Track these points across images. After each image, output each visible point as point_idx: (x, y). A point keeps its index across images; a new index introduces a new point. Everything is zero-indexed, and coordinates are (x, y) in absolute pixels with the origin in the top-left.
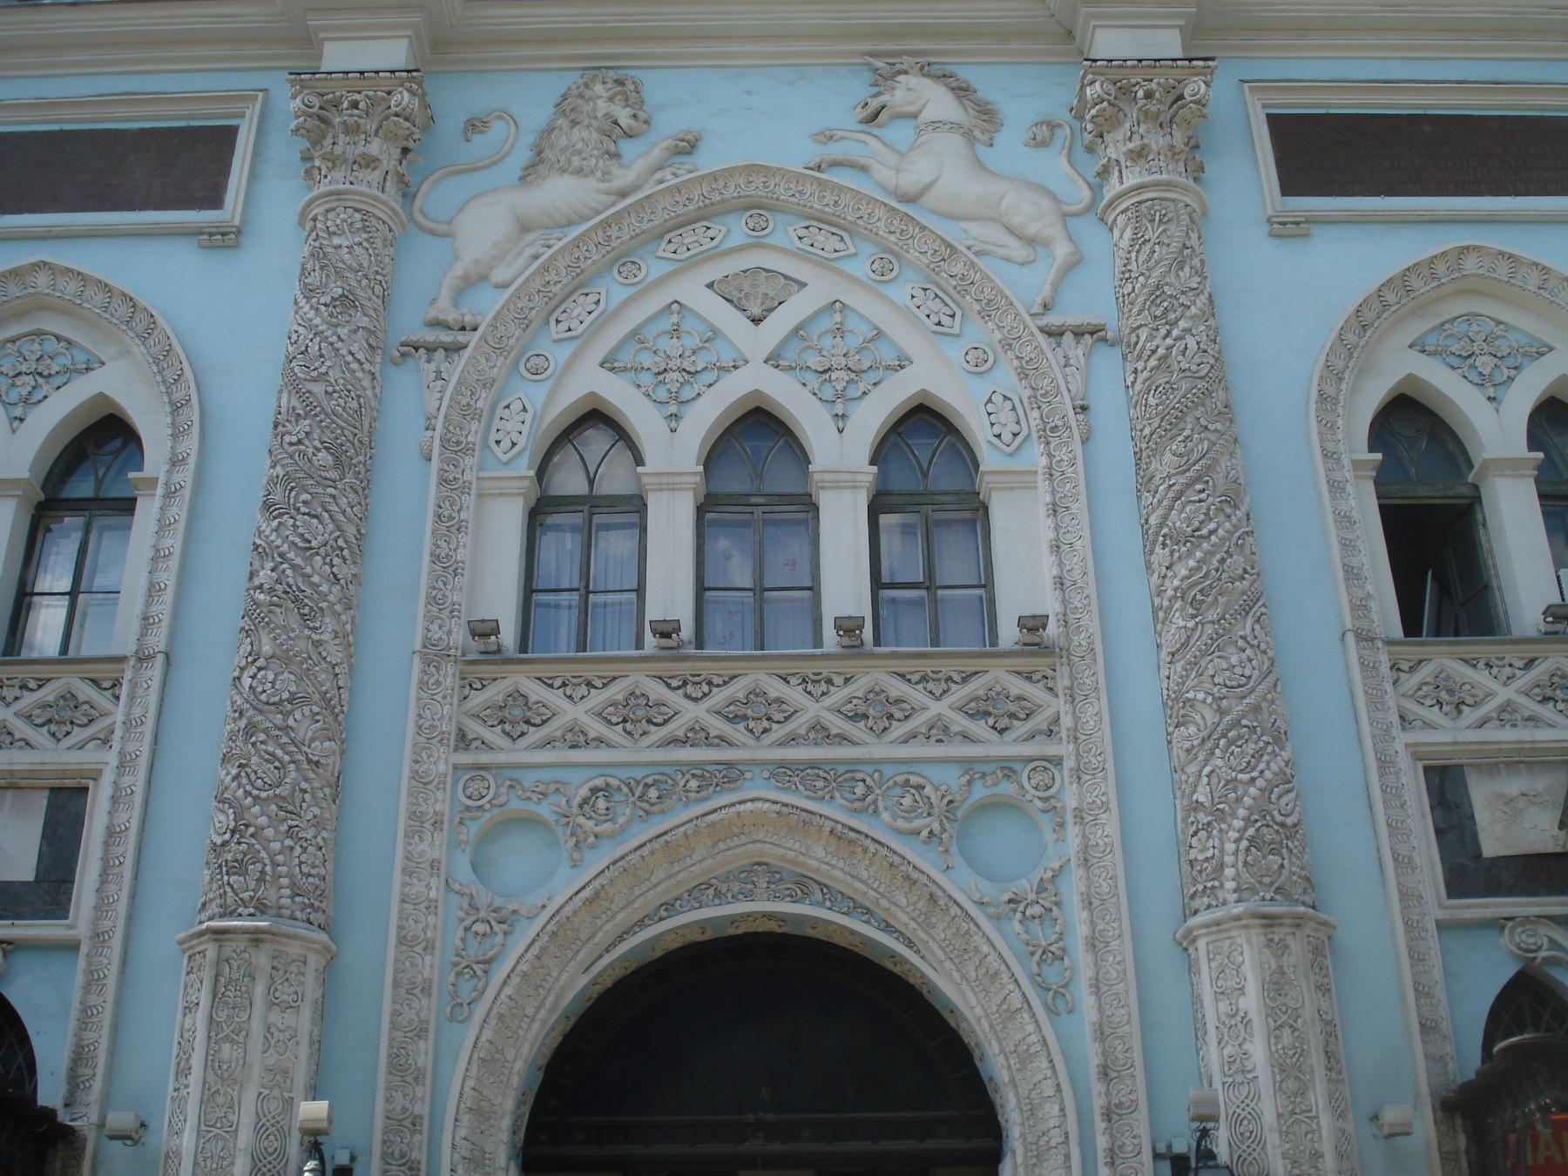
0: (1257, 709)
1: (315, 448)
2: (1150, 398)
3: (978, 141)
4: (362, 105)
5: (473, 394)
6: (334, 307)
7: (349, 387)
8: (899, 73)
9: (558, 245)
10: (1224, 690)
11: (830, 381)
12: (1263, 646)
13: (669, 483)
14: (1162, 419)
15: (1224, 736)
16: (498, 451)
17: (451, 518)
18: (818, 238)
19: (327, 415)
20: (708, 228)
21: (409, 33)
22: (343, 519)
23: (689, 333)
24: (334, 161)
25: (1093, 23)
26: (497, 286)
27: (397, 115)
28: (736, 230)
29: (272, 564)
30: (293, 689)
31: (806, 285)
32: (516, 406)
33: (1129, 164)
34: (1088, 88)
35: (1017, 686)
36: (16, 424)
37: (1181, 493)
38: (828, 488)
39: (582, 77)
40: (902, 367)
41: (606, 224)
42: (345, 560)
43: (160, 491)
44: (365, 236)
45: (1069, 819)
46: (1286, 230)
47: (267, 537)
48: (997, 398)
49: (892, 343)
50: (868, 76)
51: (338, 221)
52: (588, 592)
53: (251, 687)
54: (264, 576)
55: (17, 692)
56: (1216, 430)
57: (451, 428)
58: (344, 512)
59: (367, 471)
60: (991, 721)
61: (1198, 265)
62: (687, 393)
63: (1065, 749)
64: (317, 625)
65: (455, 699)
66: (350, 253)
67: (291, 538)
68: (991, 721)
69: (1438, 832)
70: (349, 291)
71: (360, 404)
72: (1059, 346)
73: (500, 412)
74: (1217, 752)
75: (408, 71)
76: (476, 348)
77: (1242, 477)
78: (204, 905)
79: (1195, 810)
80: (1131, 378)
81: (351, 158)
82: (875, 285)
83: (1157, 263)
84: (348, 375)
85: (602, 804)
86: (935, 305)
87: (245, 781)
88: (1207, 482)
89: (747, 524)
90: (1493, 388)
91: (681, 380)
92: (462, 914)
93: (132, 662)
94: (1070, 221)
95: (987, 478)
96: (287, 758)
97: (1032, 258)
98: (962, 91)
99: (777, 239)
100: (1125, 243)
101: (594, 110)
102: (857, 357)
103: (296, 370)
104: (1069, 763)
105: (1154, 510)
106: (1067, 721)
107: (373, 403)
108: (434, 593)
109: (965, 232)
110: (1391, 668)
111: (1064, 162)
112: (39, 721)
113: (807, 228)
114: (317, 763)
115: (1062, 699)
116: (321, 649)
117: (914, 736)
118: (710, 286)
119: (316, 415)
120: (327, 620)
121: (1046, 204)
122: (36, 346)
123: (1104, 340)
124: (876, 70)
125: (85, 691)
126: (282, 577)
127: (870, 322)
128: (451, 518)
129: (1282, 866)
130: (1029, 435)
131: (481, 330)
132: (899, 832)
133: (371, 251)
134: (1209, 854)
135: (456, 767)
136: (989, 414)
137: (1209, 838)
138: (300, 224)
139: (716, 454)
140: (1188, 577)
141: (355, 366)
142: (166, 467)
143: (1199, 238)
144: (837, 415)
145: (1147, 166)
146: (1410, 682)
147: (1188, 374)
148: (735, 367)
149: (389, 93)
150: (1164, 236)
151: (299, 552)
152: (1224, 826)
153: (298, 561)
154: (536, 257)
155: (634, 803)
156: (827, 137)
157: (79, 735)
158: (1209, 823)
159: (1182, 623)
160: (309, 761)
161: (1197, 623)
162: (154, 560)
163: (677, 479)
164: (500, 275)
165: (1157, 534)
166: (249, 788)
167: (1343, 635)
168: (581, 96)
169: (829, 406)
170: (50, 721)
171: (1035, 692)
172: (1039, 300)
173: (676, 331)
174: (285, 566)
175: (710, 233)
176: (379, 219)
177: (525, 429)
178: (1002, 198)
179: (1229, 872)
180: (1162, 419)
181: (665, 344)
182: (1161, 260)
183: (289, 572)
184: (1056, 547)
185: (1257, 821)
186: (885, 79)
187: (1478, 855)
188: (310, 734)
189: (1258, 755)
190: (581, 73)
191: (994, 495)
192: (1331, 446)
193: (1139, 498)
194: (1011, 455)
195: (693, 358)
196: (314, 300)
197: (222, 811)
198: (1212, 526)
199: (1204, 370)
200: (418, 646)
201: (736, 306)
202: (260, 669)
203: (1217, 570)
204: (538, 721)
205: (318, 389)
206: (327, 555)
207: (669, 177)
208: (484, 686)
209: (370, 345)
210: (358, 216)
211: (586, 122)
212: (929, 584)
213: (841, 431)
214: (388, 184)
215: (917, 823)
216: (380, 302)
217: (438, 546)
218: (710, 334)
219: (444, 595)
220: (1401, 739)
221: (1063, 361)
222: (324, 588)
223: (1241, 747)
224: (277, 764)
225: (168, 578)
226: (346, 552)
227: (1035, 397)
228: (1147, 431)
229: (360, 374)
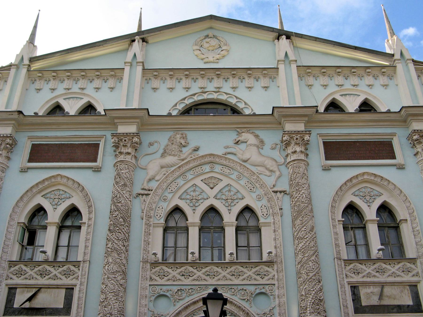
0: (315, 275)
1: (119, 218)
2: (295, 208)
3: (260, 148)
4: (127, 141)
5: (151, 204)
6: (122, 186)
7: (126, 204)
8: (243, 132)
9: (170, 172)
10: (309, 271)
11: (227, 202)
12: (317, 262)
13: (193, 225)
14: (298, 212)
15: (308, 281)
16: (157, 217)
17: (147, 232)
18: (225, 170)
19: (121, 210)
20: (201, 168)
21: (137, 124)
22: (125, 233)
23: (197, 191)
24: (121, 153)
25: (285, 122)
26: (156, 181)
27: (134, 143)
28: (207, 168)
29: (111, 243)
30: (116, 269)
31: (222, 180)
32: (161, 207)
33: (292, 154)
34: (284, 138)
35: (266, 268)
36: (55, 209)
37: (301, 229)
38: (227, 226)
39: (174, 132)
40: (243, 199)
41: (179, 167)
42: (126, 241)
43: (86, 225)
44: (128, 170)
45: (276, 297)
46: (326, 169)
47: (110, 237)
48: (263, 206)
49: (241, 194)
50: (236, 133)
51: (123, 167)
52: (176, 247)
53: (108, 269)
54: (110, 245)
55: (58, 268)
56: (309, 215)
57: (147, 212)
58: (125, 232)
59: (130, 222)
60: (261, 276)
61: (306, 178)
62: (197, 205)
63: (276, 283)
64: (121, 256)
65: (149, 271)
66: (125, 174)
67: (115, 237)
68: (261, 276)
69: (353, 300)
70: (125, 183)
71: (128, 208)
72: (276, 195)
73: (157, 209)
74: (307, 284)
75: (137, 133)
76: (152, 195)
77: (314, 225)
78: (99, 314)
79: (302, 296)
80: (291, 203)
81: (125, 152)
82: (237, 181)
83: (297, 177)
84: (126, 202)
85: (180, 293)
86: (250, 185)
87: (107, 289)
88: (307, 226)
89: (209, 233)
90: (369, 204)
91: (196, 202)
92: (152, 315)
93: (82, 262)
94: (280, 166)
95: (261, 224)
96: (116, 284)
97: (271, 175)
98: (257, 136)
99: (216, 170)
100: (291, 172)
101: (177, 141)
102: (233, 197)
103: (115, 200)
104: (276, 285)
105: (295, 232)
106: (276, 277)
107: (131, 207)
108: (144, 248)
109: (257, 169)
110: (344, 265)
111: (278, 153)
112: (63, 274)
113: (223, 168)
114: (122, 285)
115: (275, 272)
116: (122, 261)
117: (244, 279)
118: (202, 180)
119: (119, 211)
120: (123, 255)
121: (274, 163)
122: (58, 192)
123: (286, 193)
124: (238, 131)
125: (72, 268)
126: (114, 246)
127: (236, 189)
128: (147, 232)
129: (319, 308)
130: (270, 214)
131: (153, 191)
132: (242, 299)
133: (129, 174)
134: (304, 305)
135: (150, 285)
136: (261, 210)
137: (304, 302)
138: (114, 166)
139: (203, 217)
140: (302, 247)
141: (127, 199)
142: (88, 220)
143: (307, 171)
144: (229, 210)
145: (296, 155)
146: (348, 268)
147: (303, 202)
148: (207, 199)
149: (133, 138)
150: (299, 171)
151: (117, 240)
152: (307, 300)
153: (117, 242)
154: (165, 174)
155: (187, 293)
156: (227, 147)
157: (71, 277)
158: (305, 299)
159: (300, 257)
160: (120, 284)
161: (303, 257)
162: (86, 240)
163: (195, 224)
164: (157, 178)
165: (296, 237)
166: (108, 290)
167: (334, 259)
168: (174, 137)
169: (227, 207)
170: (65, 274)
171: (270, 269)
172: (272, 185)
173: (194, 191)
174: (114, 243)
175: (202, 169)
176: (131, 166)
177: (163, 212)
178: (265, 161)
179: (308, 309)
180: (298, 212)
181: (192, 193)
182: (298, 177)
183: (115, 245)
184: (275, 239)
185: (314, 299)
186: (239, 134)
187: (361, 305)
188: (120, 279)
189: (315, 284)
190: (173, 132)
191: (262, 228)
192: (333, 217)
193: (292, 229)
194: (266, 219)
195: (198, 197)
196: (118, 185)
197: (102, 294)
198: (307, 236)
199: (307, 201)
200: (141, 260)
201: (207, 185)
202: (109, 265)
203: (308, 245)
204: (166, 275)
205: (120, 205)
206: (122, 241)
207: (193, 156)
208: (155, 268)
209: (130, 194)
210: (127, 166)
211: (175, 144)
212: (248, 246)
213: (230, 213)
214: (133, 158)
215: (245, 298)
216: (132, 185)
217: (145, 238)
218: (202, 191)
219: (146, 249)
220: (346, 280)
221: (277, 198)
222: (122, 248)
223: (311, 283)
224: (114, 285)
225: (89, 244)
226: (126, 240)
227: (271, 206)
228: (294, 215)
229: (128, 201)
